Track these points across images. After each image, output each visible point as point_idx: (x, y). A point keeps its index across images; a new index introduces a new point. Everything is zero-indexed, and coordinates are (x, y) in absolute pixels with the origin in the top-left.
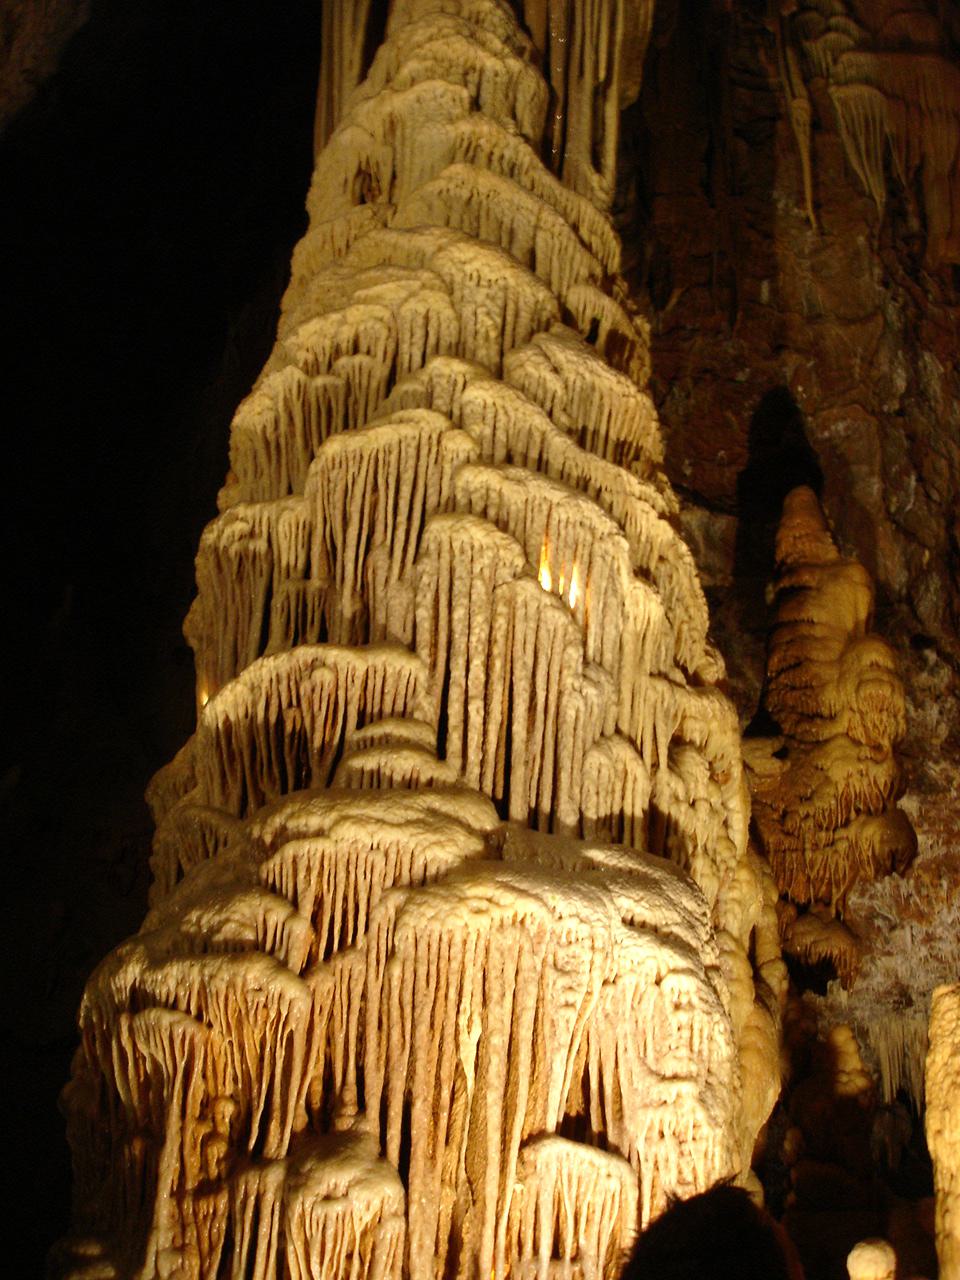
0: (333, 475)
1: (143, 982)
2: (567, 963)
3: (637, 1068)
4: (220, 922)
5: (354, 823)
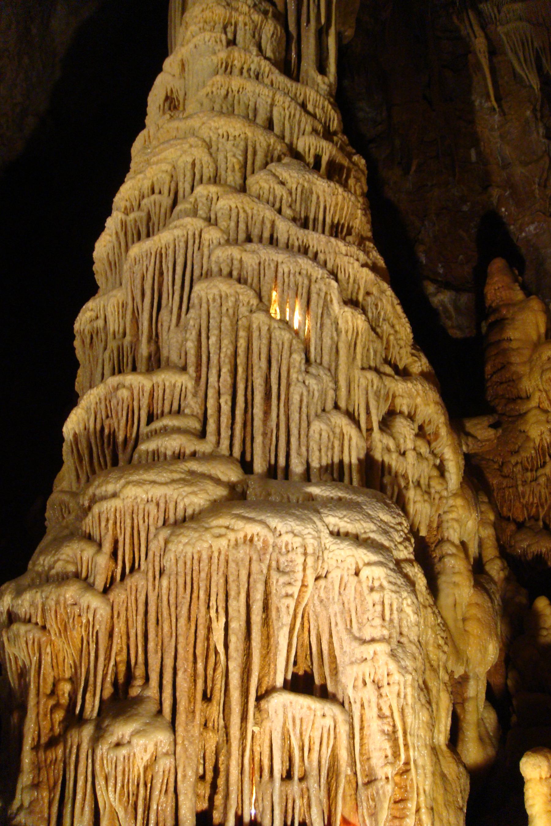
2: (287, 566)
3: (345, 636)
5: (134, 485)
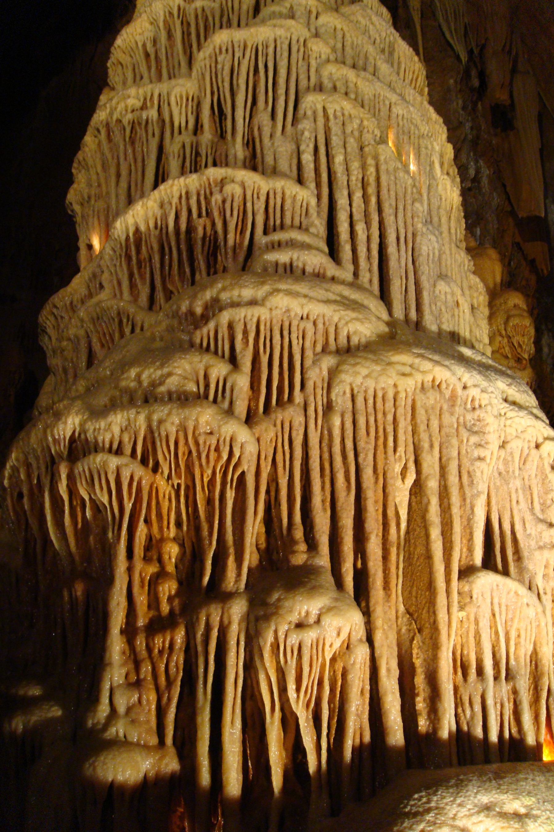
0: (219, 59)
1: (83, 431)
2: (474, 425)
4: (162, 376)
5: (286, 295)
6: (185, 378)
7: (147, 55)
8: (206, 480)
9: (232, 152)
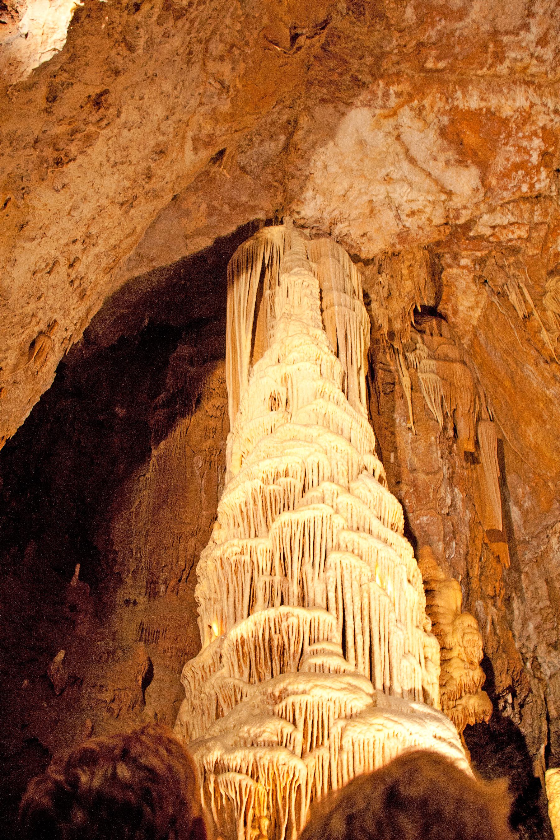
0: (284, 530)
6: (272, 734)
7: (242, 511)
8: (282, 787)
9: (291, 590)
